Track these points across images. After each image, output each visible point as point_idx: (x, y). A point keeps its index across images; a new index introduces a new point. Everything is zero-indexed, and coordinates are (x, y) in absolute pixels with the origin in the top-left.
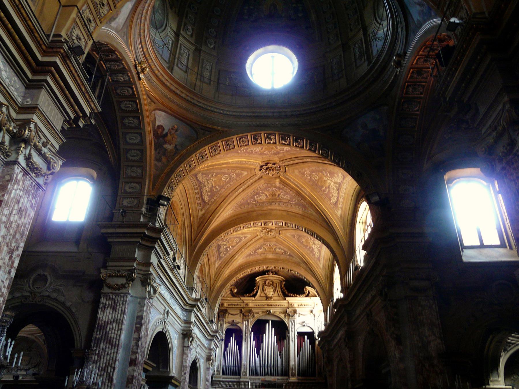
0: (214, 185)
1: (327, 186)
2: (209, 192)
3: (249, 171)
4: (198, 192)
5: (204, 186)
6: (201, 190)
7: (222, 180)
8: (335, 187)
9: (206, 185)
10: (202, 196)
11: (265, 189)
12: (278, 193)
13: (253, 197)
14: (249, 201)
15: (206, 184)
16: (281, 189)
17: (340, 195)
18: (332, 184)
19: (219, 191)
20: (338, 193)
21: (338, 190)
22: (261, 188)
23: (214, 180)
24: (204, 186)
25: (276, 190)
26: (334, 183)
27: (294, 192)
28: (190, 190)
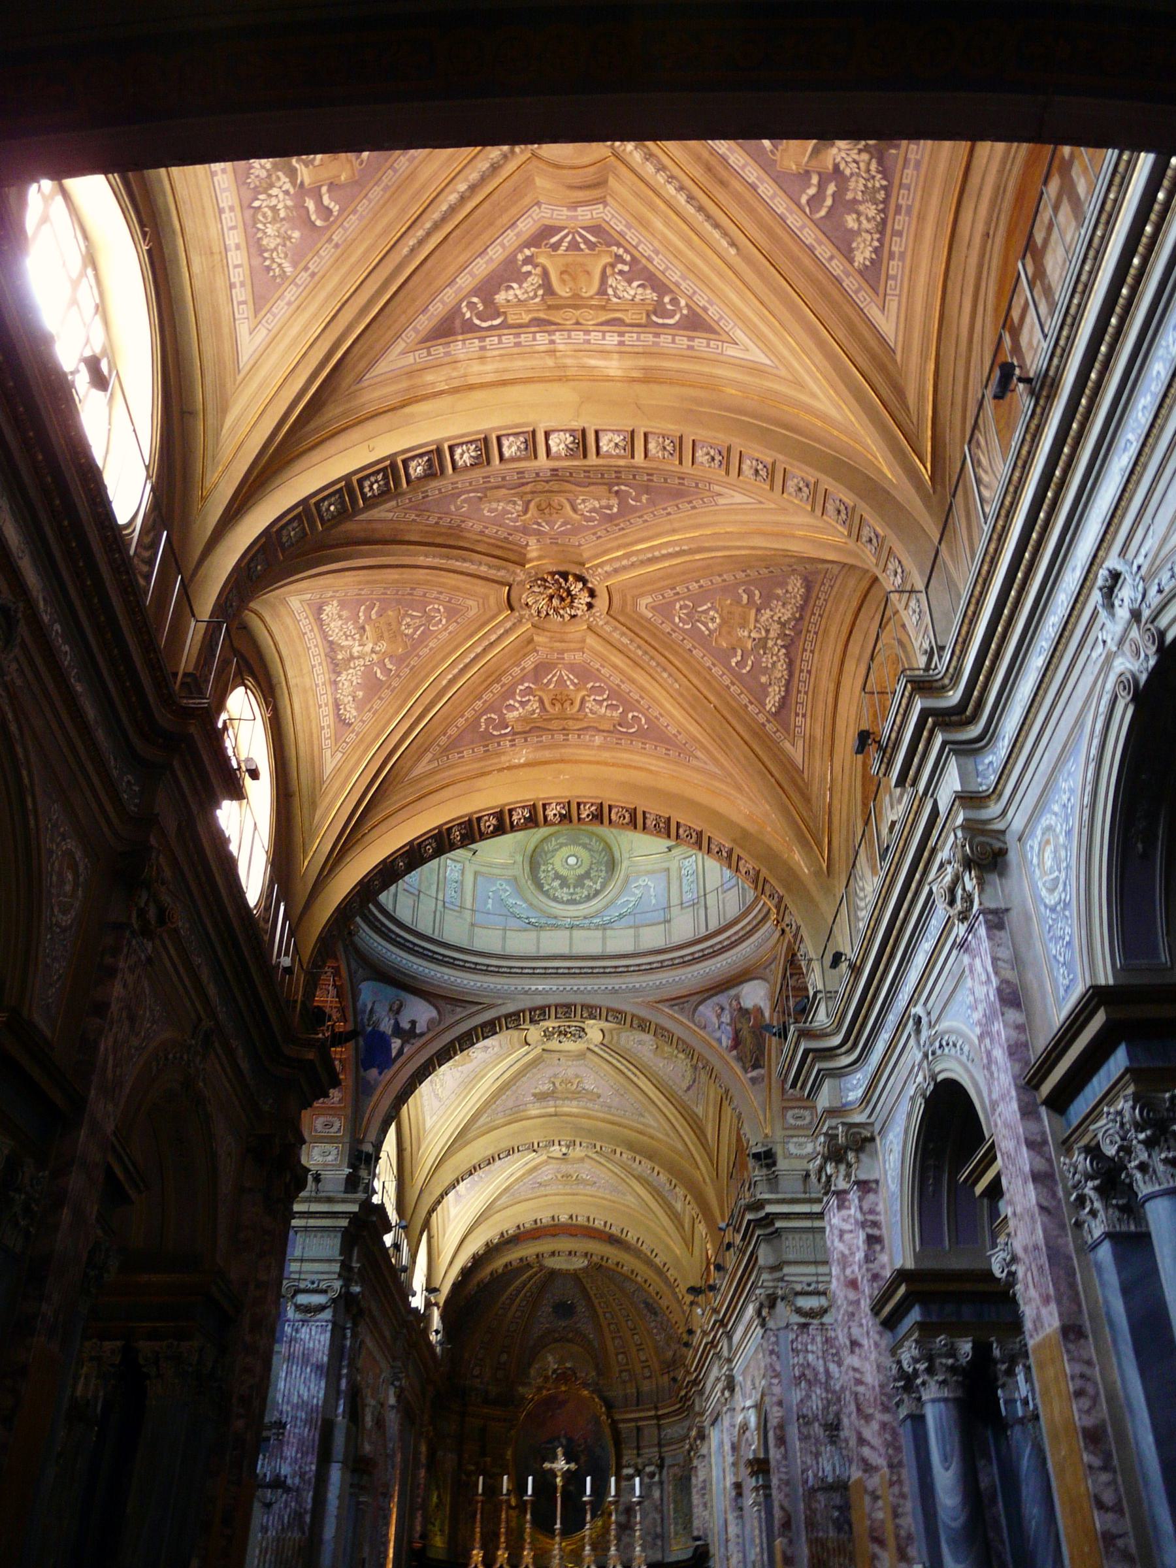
0: (753, 612)
1: (367, 627)
2: (778, 598)
3: (629, 609)
4: (813, 614)
5: (783, 625)
6: (801, 618)
7: (721, 616)
8: (344, 643)
9: (776, 626)
10: (806, 598)
11: (576, 530)
12: (529, 515)
13: (625, 510)
14: (644, 498)
15: (775, 629)
16: (516, 529)
17: (318, 636)
18: (356, 650)
19: (744, 583)
20: (325, 636)
21: (331, 643)
22: (594, 534)
23: (746, 633)
24: (783, 625)
25: (539, 524)
26: (352, 658)
27: (469, 531)
28: (833, 630)
